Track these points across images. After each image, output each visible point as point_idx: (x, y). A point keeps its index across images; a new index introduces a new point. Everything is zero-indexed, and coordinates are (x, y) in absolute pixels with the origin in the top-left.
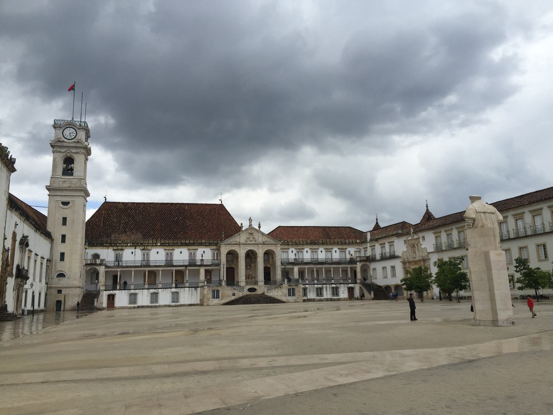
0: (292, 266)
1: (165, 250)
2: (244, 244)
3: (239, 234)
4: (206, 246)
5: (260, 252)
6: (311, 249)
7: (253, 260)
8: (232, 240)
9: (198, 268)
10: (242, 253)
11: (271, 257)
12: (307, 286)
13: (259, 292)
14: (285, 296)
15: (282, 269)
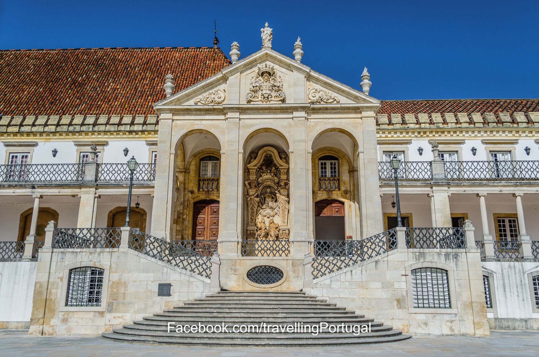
0: (427, 190)
1: (7, 145)
2: (242, 110)
3: (225, 79)
4: (130, 132)
5: (300, 138)
6: (484, 142)
7: (284, 177)
8: (198, 96)
9: (75, 191)
10: (232, 139)
11: (345, 169)
12: (491, 266)
13: (291, 283)
14: (400, 302)
15: (384, 197)
